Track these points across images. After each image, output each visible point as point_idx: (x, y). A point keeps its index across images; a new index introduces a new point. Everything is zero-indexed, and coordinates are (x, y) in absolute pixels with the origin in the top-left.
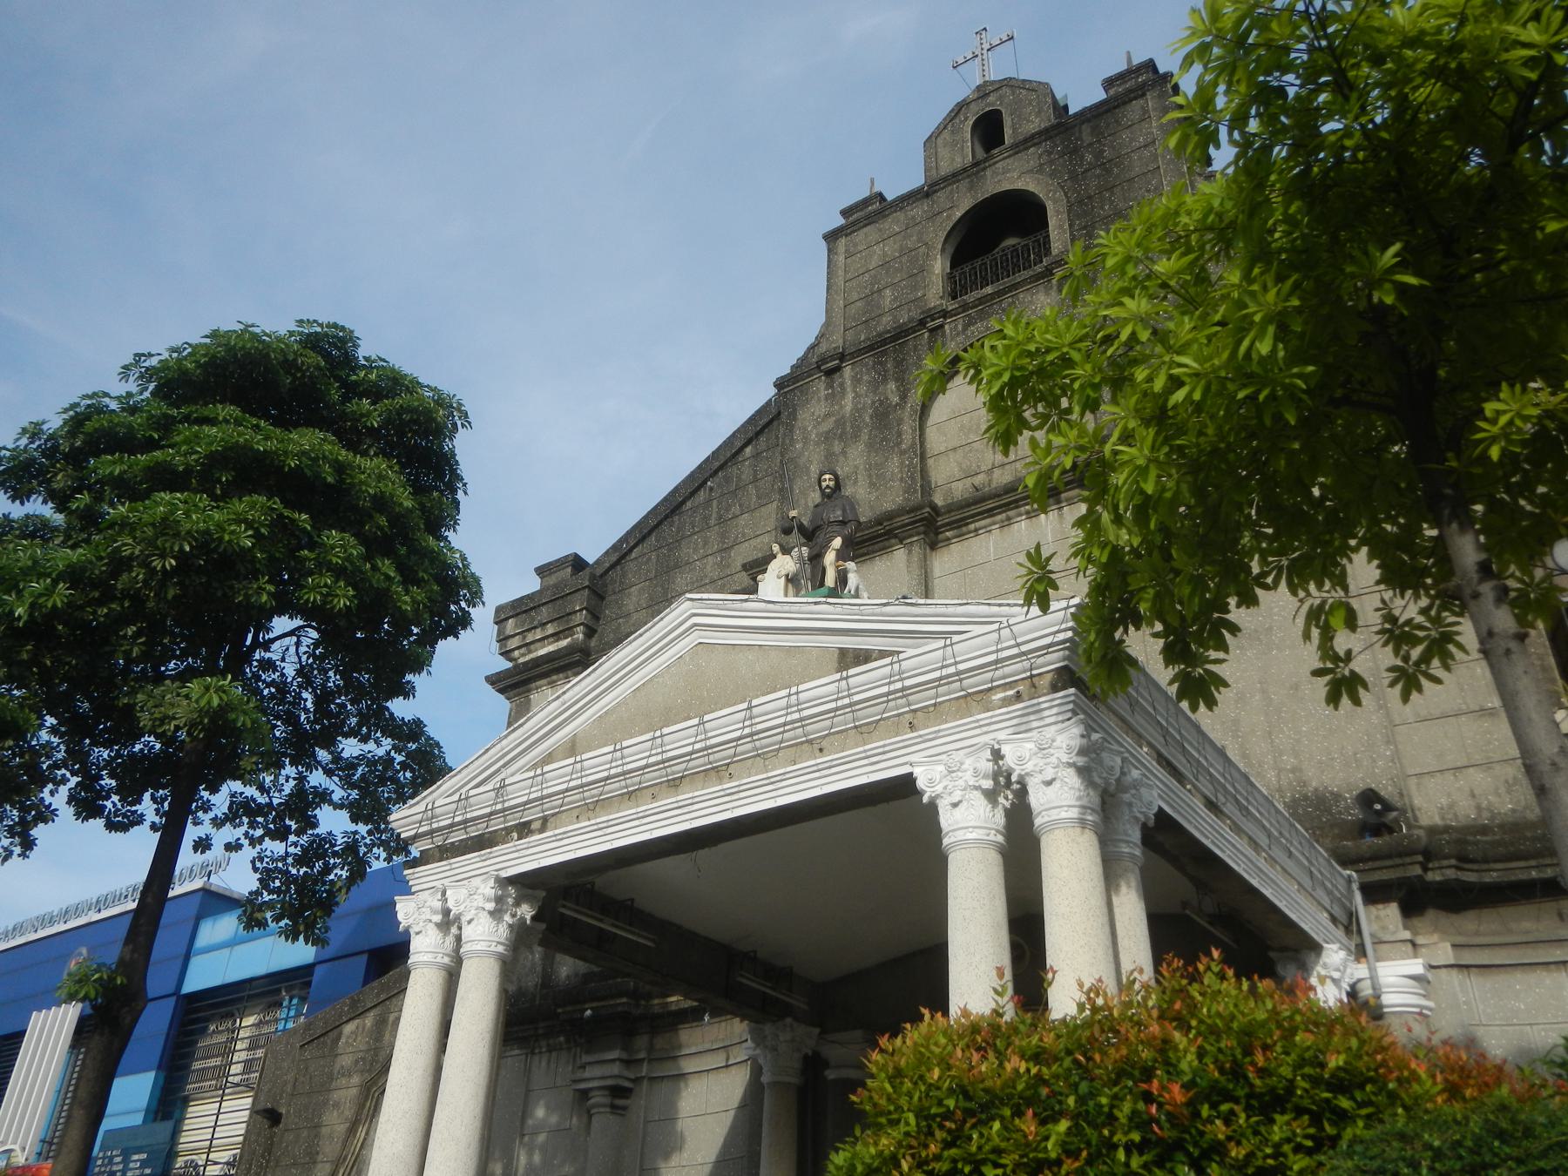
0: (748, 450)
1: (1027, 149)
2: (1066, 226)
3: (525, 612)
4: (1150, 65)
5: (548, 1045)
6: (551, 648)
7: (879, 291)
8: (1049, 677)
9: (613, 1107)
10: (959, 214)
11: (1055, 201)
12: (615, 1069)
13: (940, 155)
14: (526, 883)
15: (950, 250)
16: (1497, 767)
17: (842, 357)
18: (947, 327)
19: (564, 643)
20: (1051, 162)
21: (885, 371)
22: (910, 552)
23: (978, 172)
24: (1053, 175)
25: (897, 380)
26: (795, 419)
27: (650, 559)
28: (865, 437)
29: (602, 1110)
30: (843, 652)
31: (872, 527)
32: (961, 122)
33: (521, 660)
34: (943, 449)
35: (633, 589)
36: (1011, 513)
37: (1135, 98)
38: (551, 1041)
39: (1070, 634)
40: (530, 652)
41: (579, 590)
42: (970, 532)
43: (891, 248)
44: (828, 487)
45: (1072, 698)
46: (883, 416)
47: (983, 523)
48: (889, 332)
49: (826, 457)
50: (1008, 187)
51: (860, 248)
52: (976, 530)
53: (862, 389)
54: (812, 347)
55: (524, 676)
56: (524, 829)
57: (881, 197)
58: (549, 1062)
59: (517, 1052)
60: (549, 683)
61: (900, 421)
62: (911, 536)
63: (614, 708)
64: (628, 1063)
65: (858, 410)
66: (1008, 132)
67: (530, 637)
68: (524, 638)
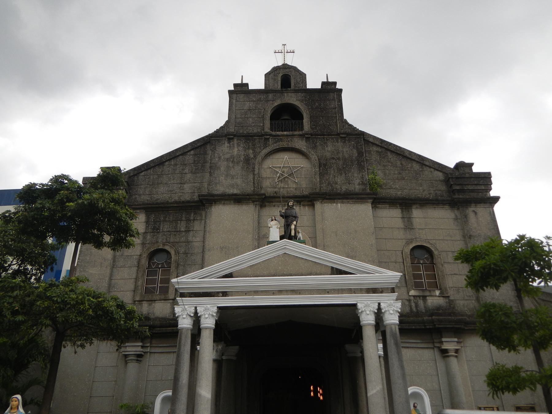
0: (192, 152)
1: (299, 93)
2: (309, 123)
4: (335, 83)
7: (247, 118)
8: (390, 289)
10: (276, 104)
11: (307, 114)
12: (140, 349)
13: (270, 81)
14: (221, 309)
15: (271, 114)
17: (235, 136)
18: (270, 139)
20: (306, 100)
21: (249, 146)
22: (256, 206)
24: (306, 104)
25: (253, 150)
26: (215, 149)
27: (150, 177)
28: (241, 164)
29: (133, 361)
30: (332, 268)
31: (245, 196)
32: (277, 73)
34: (265, 177)
35: (142, 186)
37: (332, 92)
39: (398, 281)
42: (272, 205)
43: (252, 105)
44: (291, 205)
45: (397, 295)
46: (247, 160)
47: (277, 204)
48: (251, 133)
49: (227, 166)
51: (241, 101)
53: (241, 149)
54: (221, 128)
56: (225, 294)
57: (247, 85)
58: (107, 343)
61: (254, 164)
62: (257, 202)
63: (256, 264)
64: (142, 347)
65: (238, 155)
66: (292, 84)
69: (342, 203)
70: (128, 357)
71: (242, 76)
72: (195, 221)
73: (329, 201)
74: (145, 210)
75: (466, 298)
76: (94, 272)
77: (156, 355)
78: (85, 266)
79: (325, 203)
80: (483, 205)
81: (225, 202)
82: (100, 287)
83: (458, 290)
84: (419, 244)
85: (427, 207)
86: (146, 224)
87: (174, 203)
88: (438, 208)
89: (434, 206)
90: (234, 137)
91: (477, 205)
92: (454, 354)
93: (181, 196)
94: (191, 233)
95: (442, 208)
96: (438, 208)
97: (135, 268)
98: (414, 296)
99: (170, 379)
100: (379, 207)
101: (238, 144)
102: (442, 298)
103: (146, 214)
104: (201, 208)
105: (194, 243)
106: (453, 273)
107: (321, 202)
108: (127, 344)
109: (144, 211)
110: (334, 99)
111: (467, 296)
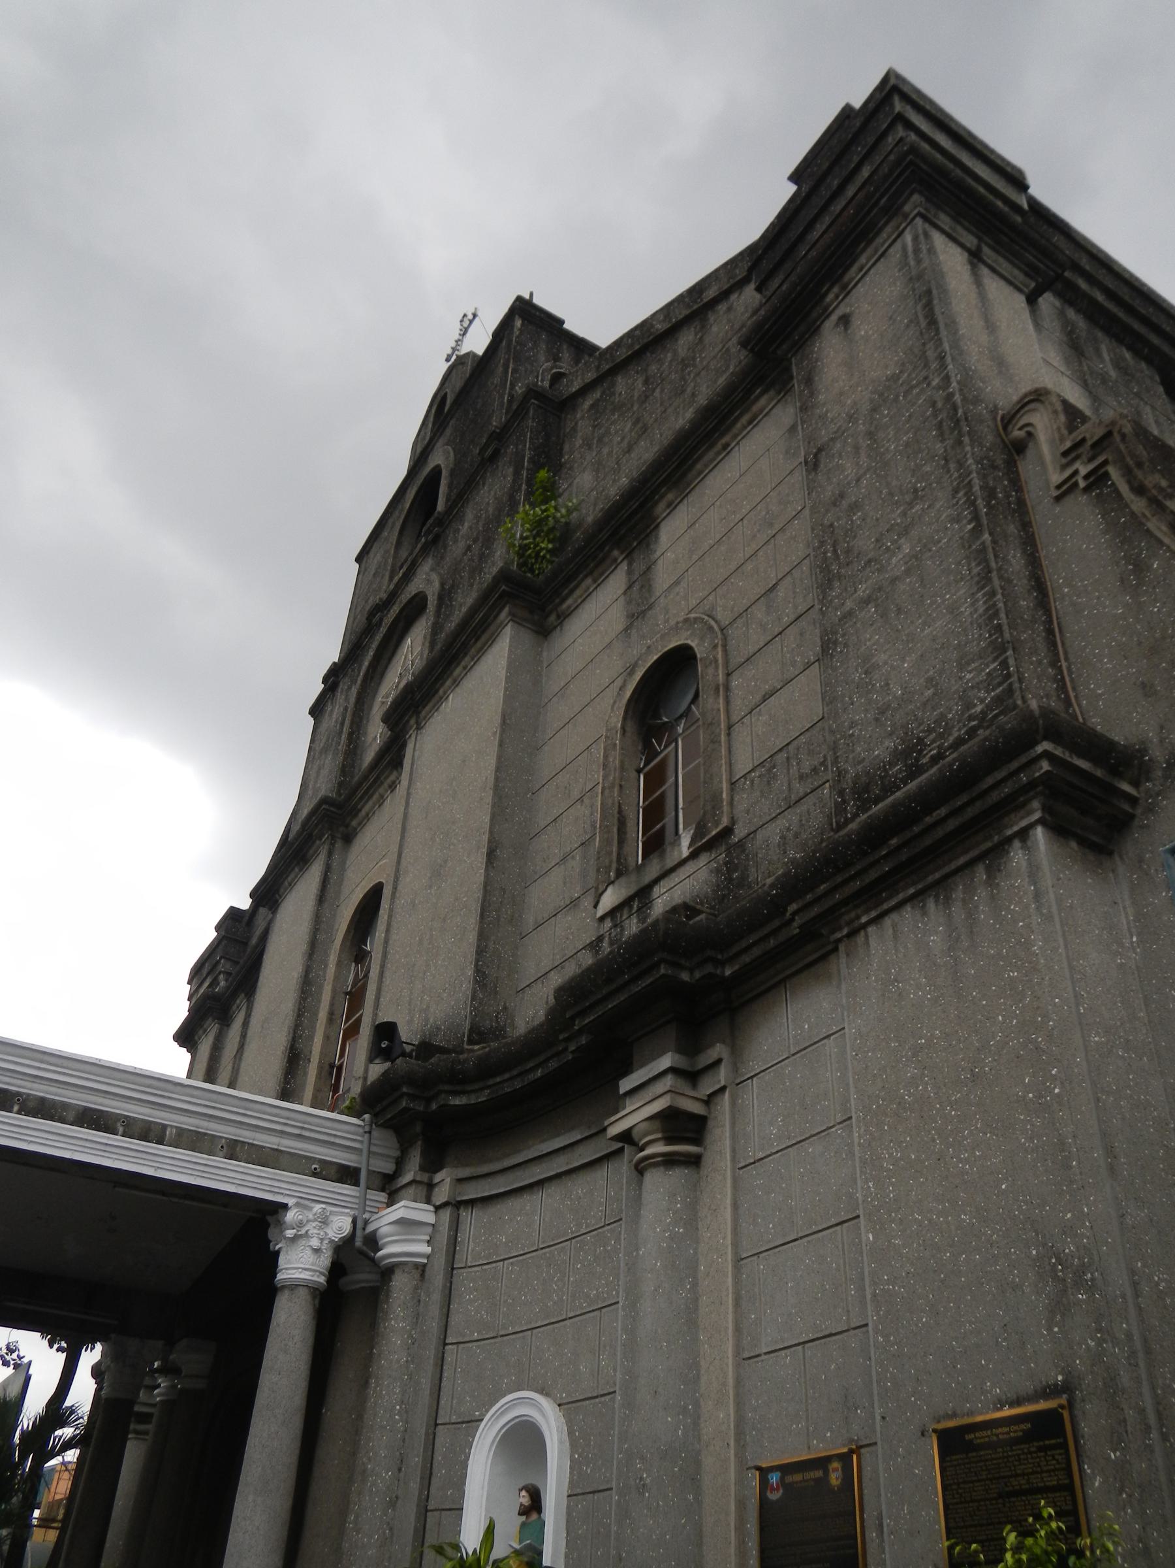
16: (567, 963)
36: (381, 790)
52: (367, 815)
69: (457, 683)
73: (431, 705)
75: (800, 788)
79: (427, 718)
80: (869, 251)
81: (289, 879)
83: (769, 770)
84: (655, 657)
85: (700, 473)
88: (739, 438)
89: (719, 446)
91: (846, 278)
92: (660, 1148)
95: (750, 422)
96: (736, 436)
98: (612, 913)
100: (569, 607)
102: (704, 859)
106: (758, 697)
107: (418, 723)
111: (802, 777)
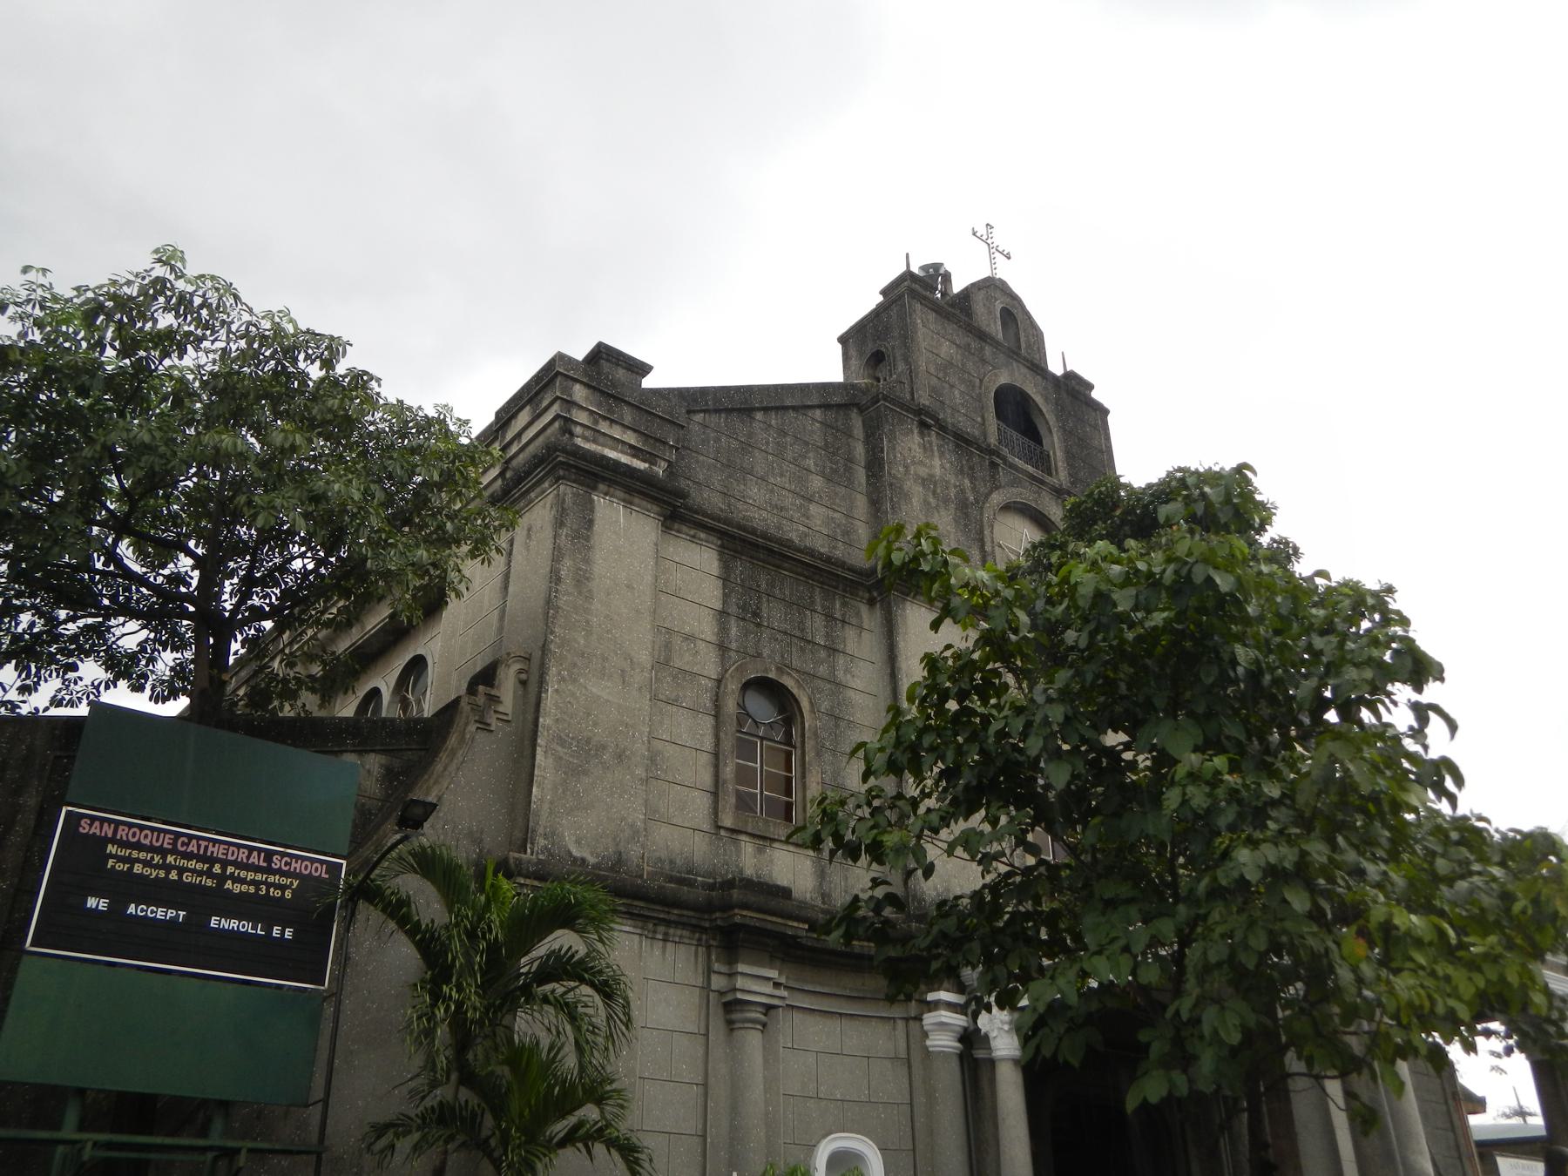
3: (602, 393)
5: (666, 934)
6: (625, 459)
9: (764, 1025)
12: (768, 988)
19: (642, 465)
23: (1012, 358)
33: (579, 441)
38: (671, 931)
40: (595, 441)
41: (674, 423)
50: (1030, 392)
55: (607, 474)
59: (627, 929)
60: (624, 501)
67: (604, 427)
68: (596, 422)
70: (742, 1011)
71: (907, 254)
72: (847, 626)
74: (719, 538)
76: (604, 695)
77: (797, 1016)
78: (575, 665)
82: (628, 753)
86: (724, 586)
87: (807, 554)
90: (934, 426)
93: (806, 535)
94: (841, 660)
97: (707, 717)
99: (839, 1097)
101: (939, 447)
103: (721, 554)
104: (861, 593)
105: (851, 693)
108: (741, 968)
109: (719, 542)
110: (1095, 427)
